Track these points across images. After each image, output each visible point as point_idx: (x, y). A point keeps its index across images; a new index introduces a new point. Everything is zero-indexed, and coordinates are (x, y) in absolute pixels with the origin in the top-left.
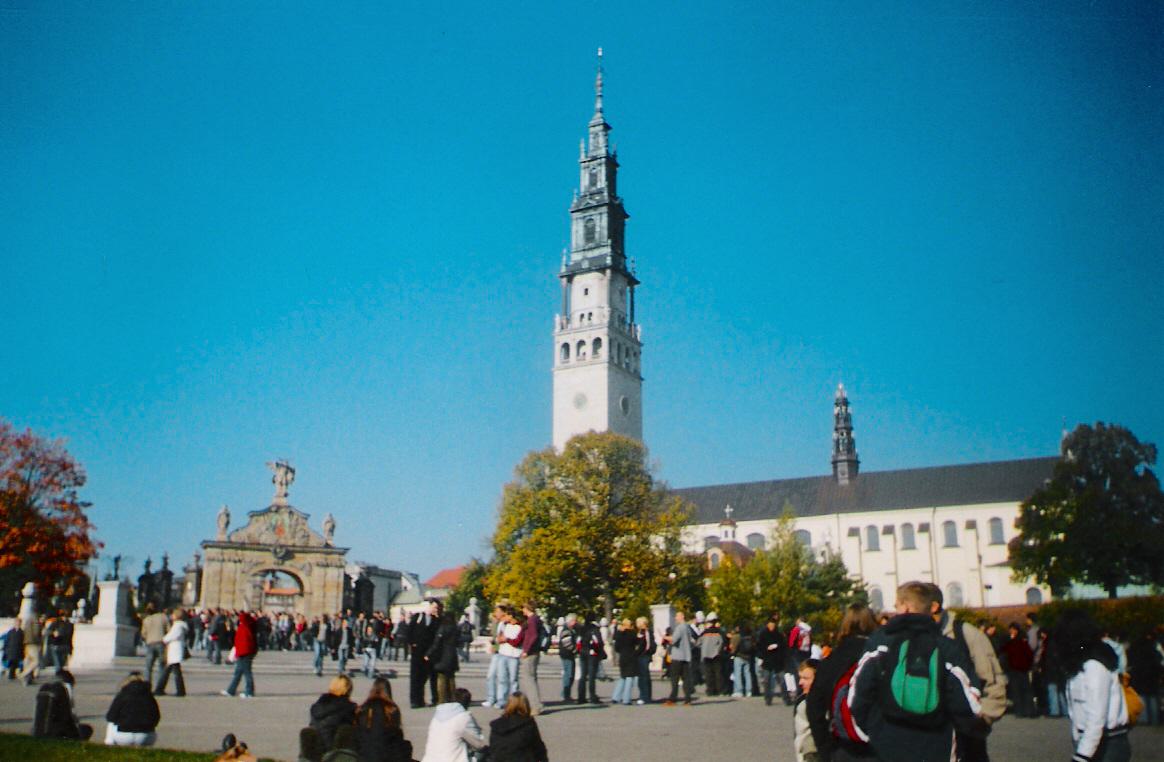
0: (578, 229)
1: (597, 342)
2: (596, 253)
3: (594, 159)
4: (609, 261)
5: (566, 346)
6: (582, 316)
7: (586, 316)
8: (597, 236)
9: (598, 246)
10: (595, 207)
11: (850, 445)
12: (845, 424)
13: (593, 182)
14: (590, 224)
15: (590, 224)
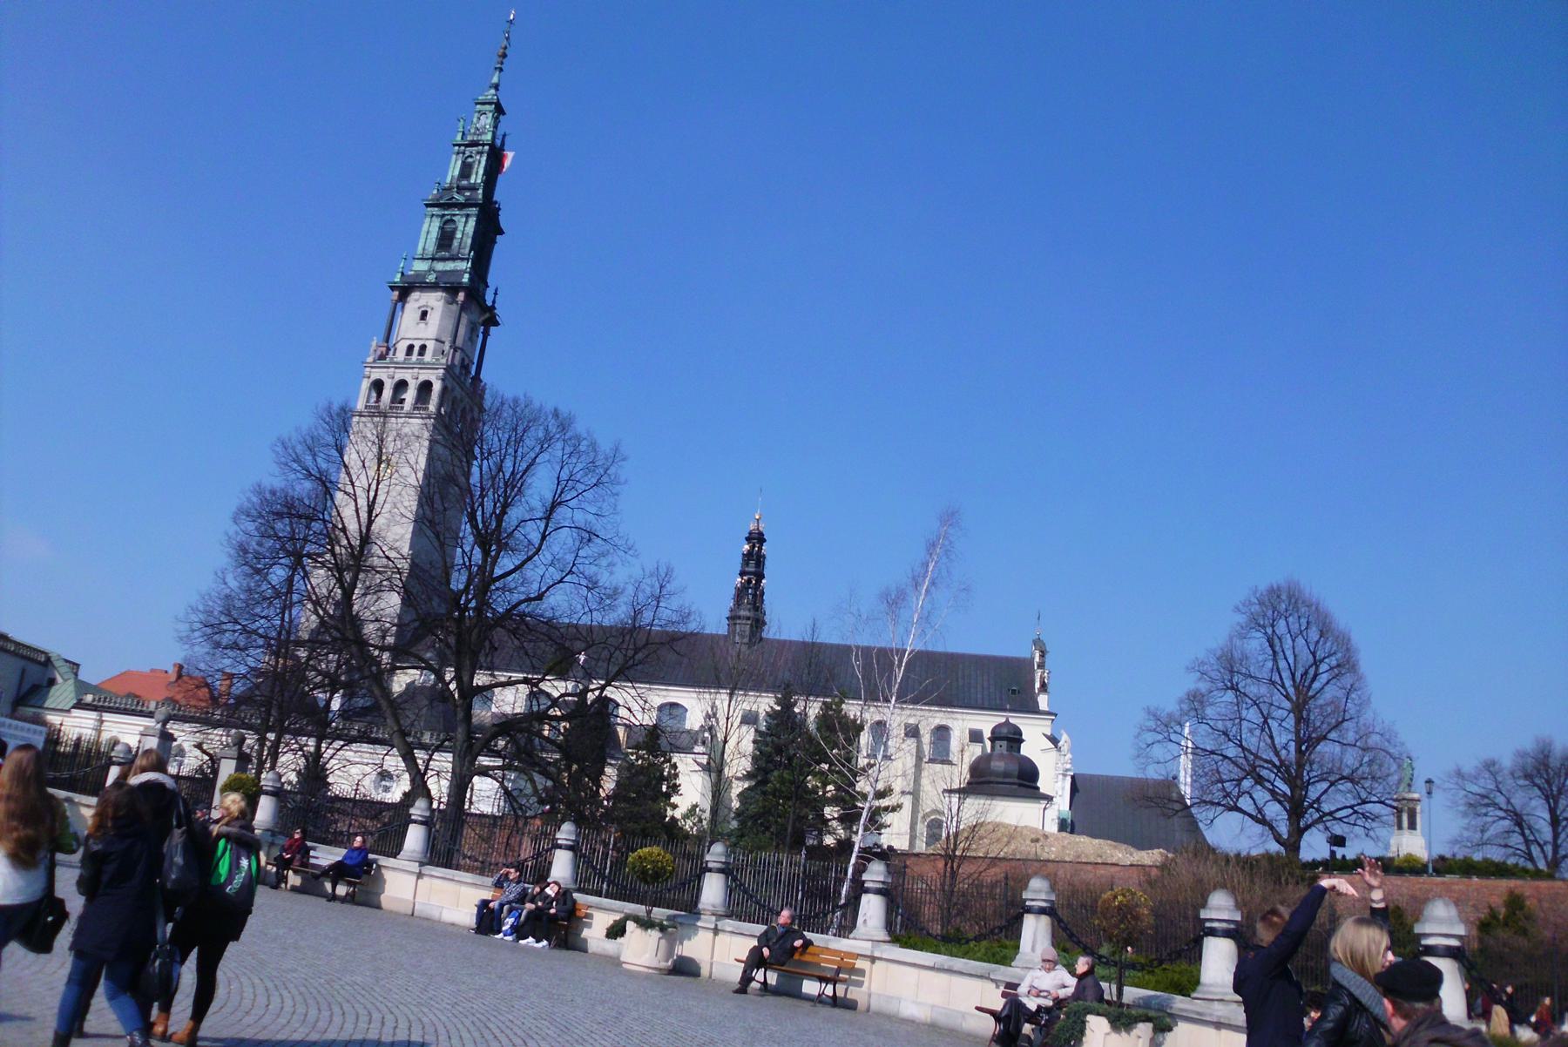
0: (430, 230)
1: (425, 387)
2: (450, 266)
3: (474, 144)
4: (466, 278)
5: (378, 386)
6: (411, 348)
7: (416, 349)
8: (456, 243)
9: (453, 259)
10: (461, 206)
11: (758, 597)
12: (754, 563)
13: (466, 170)
14: (449, 227)
15: (449, 227)
